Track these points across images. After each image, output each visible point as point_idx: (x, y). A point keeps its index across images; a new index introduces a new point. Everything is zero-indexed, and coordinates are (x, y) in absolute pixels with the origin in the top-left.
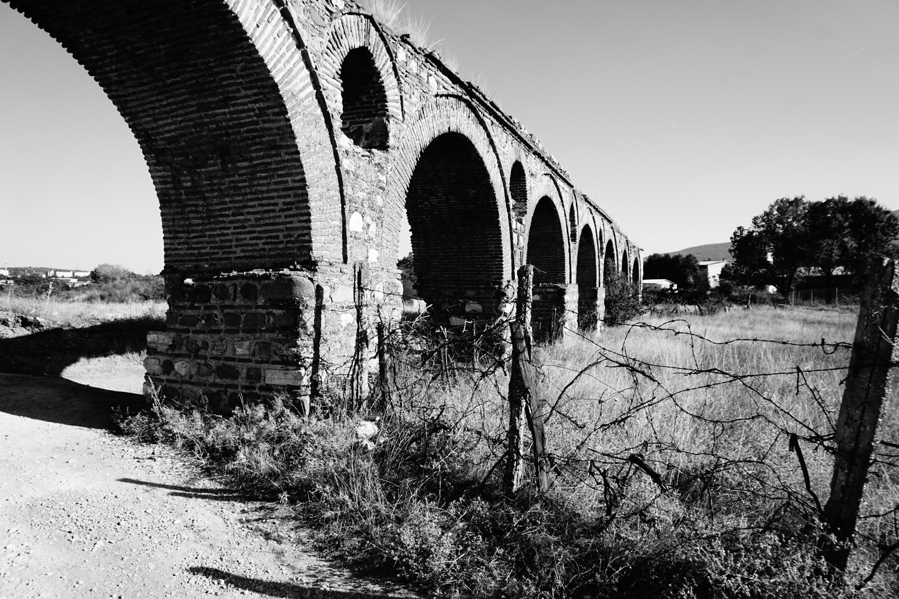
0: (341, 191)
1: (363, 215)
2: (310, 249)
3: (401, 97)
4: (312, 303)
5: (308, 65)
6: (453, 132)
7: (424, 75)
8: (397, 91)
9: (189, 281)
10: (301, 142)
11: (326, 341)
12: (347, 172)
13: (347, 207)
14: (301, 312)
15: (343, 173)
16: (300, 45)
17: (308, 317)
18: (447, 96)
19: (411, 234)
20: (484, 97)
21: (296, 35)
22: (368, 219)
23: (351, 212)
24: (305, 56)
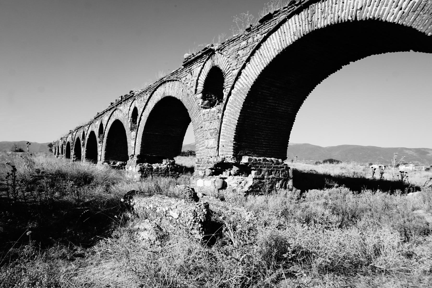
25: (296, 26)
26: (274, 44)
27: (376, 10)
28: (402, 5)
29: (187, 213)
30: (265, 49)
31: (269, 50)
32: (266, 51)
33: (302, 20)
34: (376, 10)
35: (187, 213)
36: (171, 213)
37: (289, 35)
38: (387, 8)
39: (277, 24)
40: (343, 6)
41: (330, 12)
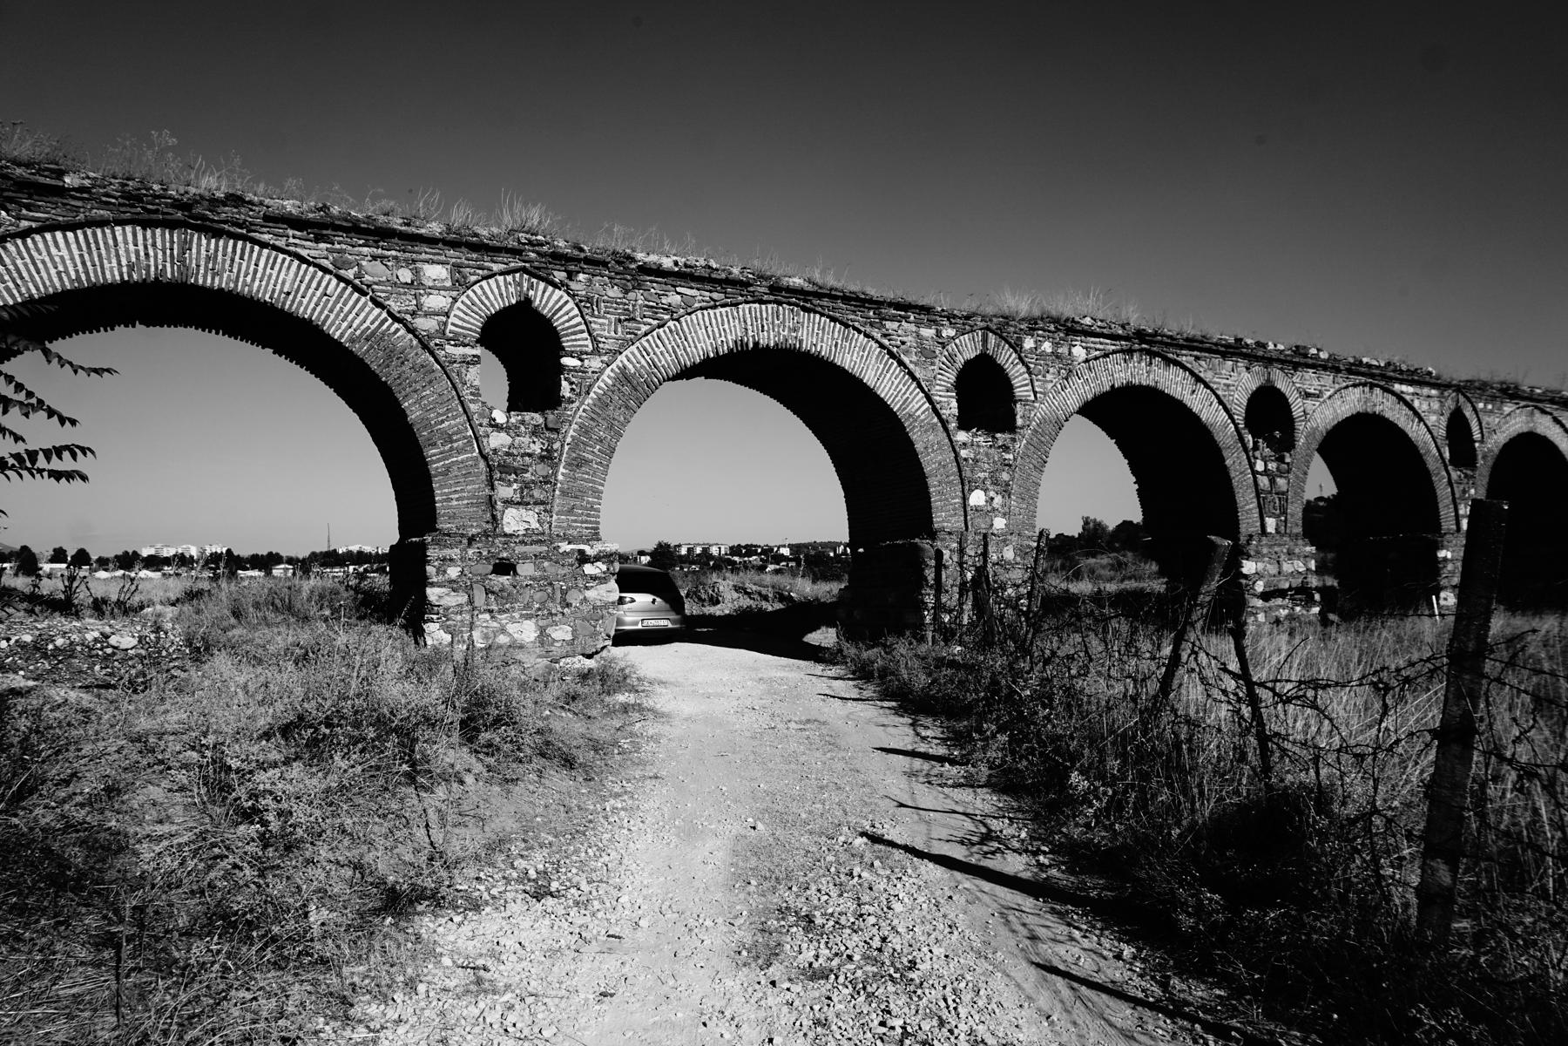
0: (961, 476)
1: (986, 491)
2: (932, 522)
3: (1032, 381)
4: (933, 563)
5: (923, 390)
6: (1119, 388)
7: (1063, 350)
8: (1026, 376)
9: (861, 550)
10: (919, 447)
11: (947, 592)
12: (966, 460)
13: (967, 488)
14: (923, 570)
15: (961, 461)
16: (914, 378)
17: (930, 574)
18: (1106, 356)
19: (1136, 486)
20: (1170, 337)
21: (911, 374)
22: (992, 494)
23: (971, 491)
24: (919, 386)
25: (137, 253)
26: (57, 259)
27: (314, 309)
28: (352, 321)
29: (166, 633)
30: (23, 258)
31: (40, 266)
32: (26, 265)
33: (154, 245)
34: (314, 309)
35: (166, 633)
36: (113, 640)
37: (114, 261)
38: (332, 316)
39: (81, 217)
40: (255, 272)
41: (227, 267)
